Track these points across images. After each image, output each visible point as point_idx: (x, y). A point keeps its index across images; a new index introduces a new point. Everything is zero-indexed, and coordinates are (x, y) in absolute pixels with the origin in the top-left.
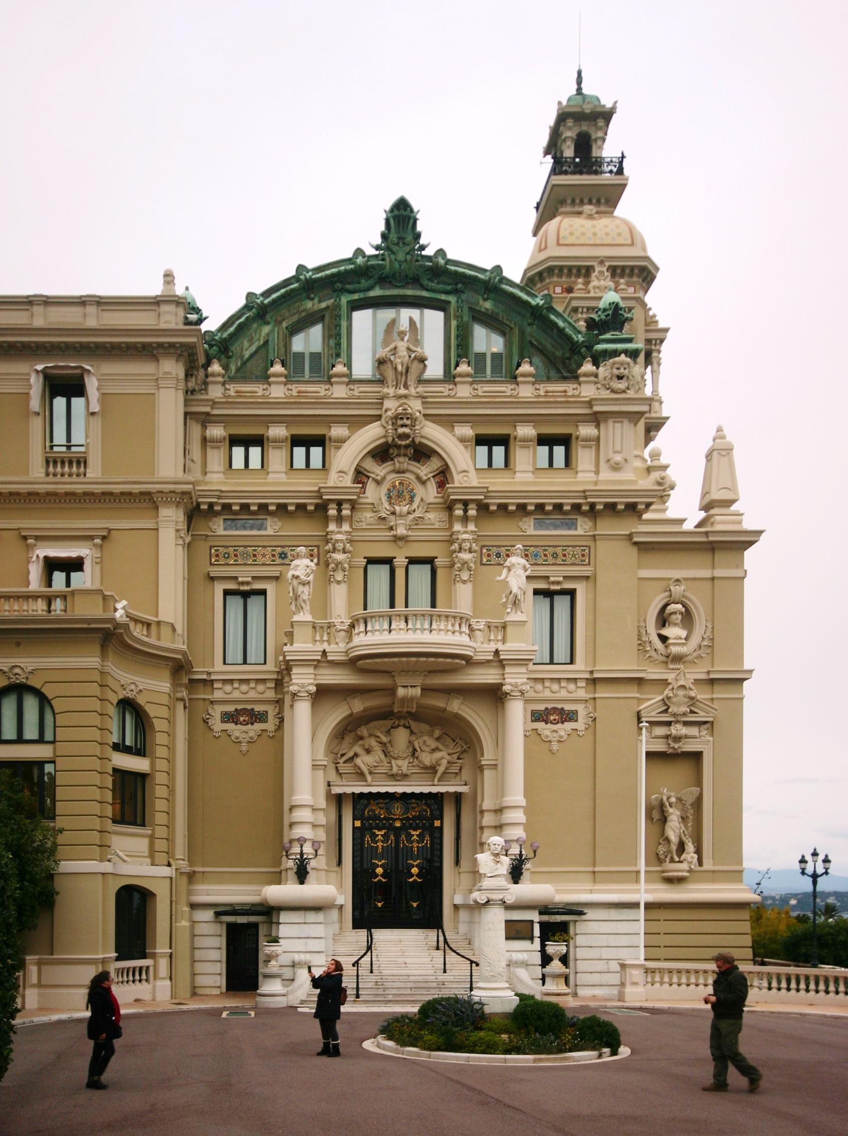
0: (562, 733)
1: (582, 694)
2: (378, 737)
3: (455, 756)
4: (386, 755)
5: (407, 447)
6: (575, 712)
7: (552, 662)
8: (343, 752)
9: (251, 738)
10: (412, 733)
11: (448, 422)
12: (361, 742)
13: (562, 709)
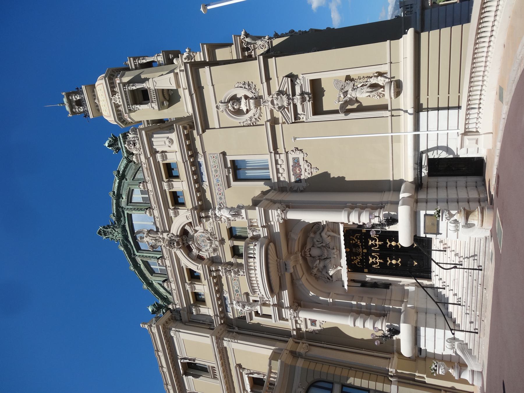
5: (183, 240)
6: (294, 159)
10: (313, 246)
11: (170, 221)
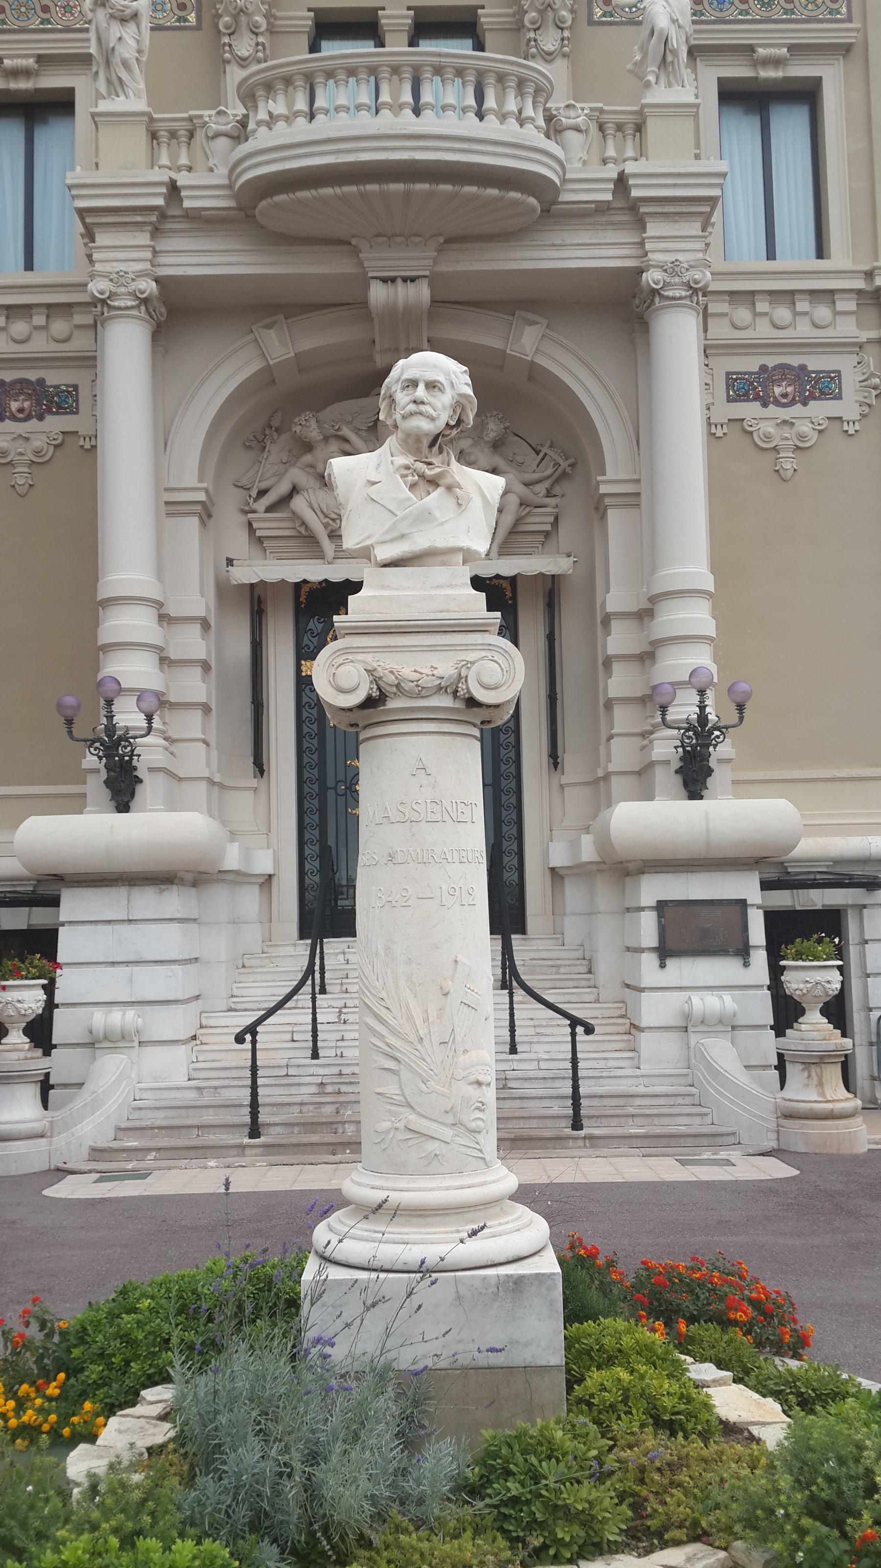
0: (805, 428)
1: (848, 329)
2: (346, 440)
3: (541, 488)
8: (264, 485)
9: (37, 453)
12: (308, 458)
13: (803, 368)
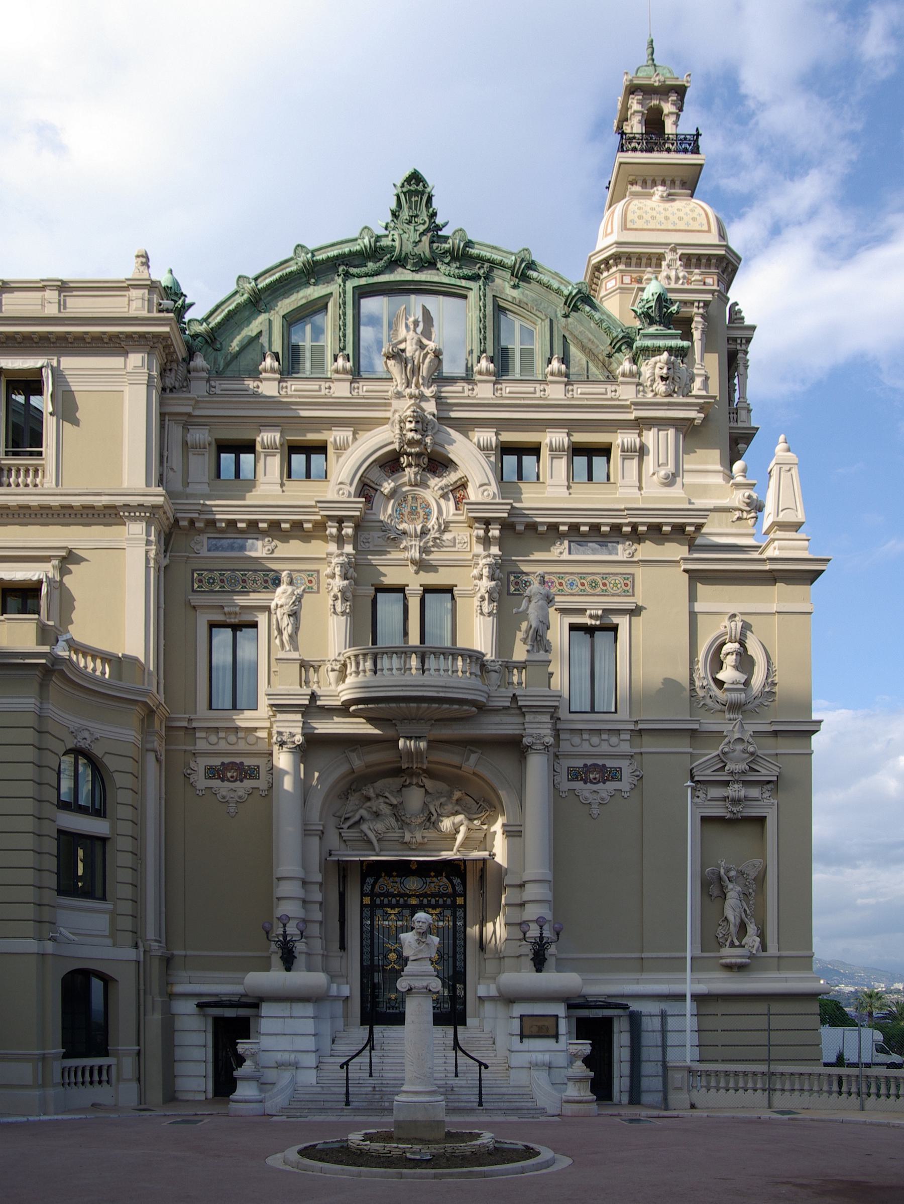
2: (386, 797)
4: (397, 820)
7: (593, 711)
8: (347, 816)
9: (240, 797)
10: (426, 792)
12: (368, 804)
13: (604, 765)
